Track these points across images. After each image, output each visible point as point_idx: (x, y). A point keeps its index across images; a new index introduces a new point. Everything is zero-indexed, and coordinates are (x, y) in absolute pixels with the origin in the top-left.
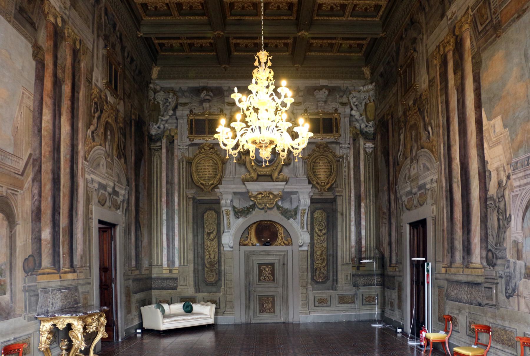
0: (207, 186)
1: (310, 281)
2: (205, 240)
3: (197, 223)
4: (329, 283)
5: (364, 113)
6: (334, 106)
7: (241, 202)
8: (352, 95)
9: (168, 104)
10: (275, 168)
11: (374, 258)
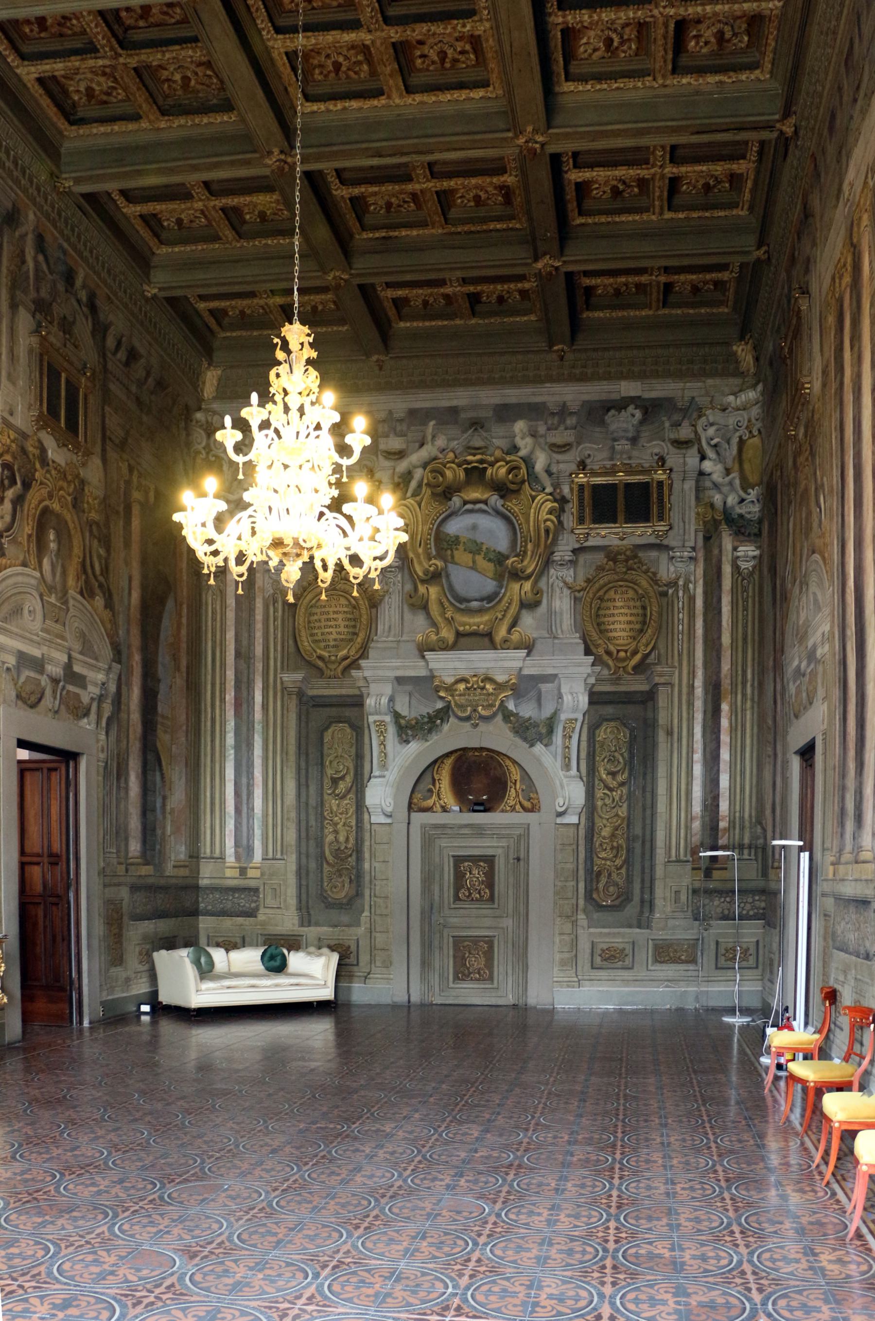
1: (581, 902)
2: (326, 797)
3: (307, 755)
4: (632, 910)
5: (736, 467)
6: (656, 450)
7: (413, 702)
8: (704, 419)
10: (500, 616)
11: (750, 847)
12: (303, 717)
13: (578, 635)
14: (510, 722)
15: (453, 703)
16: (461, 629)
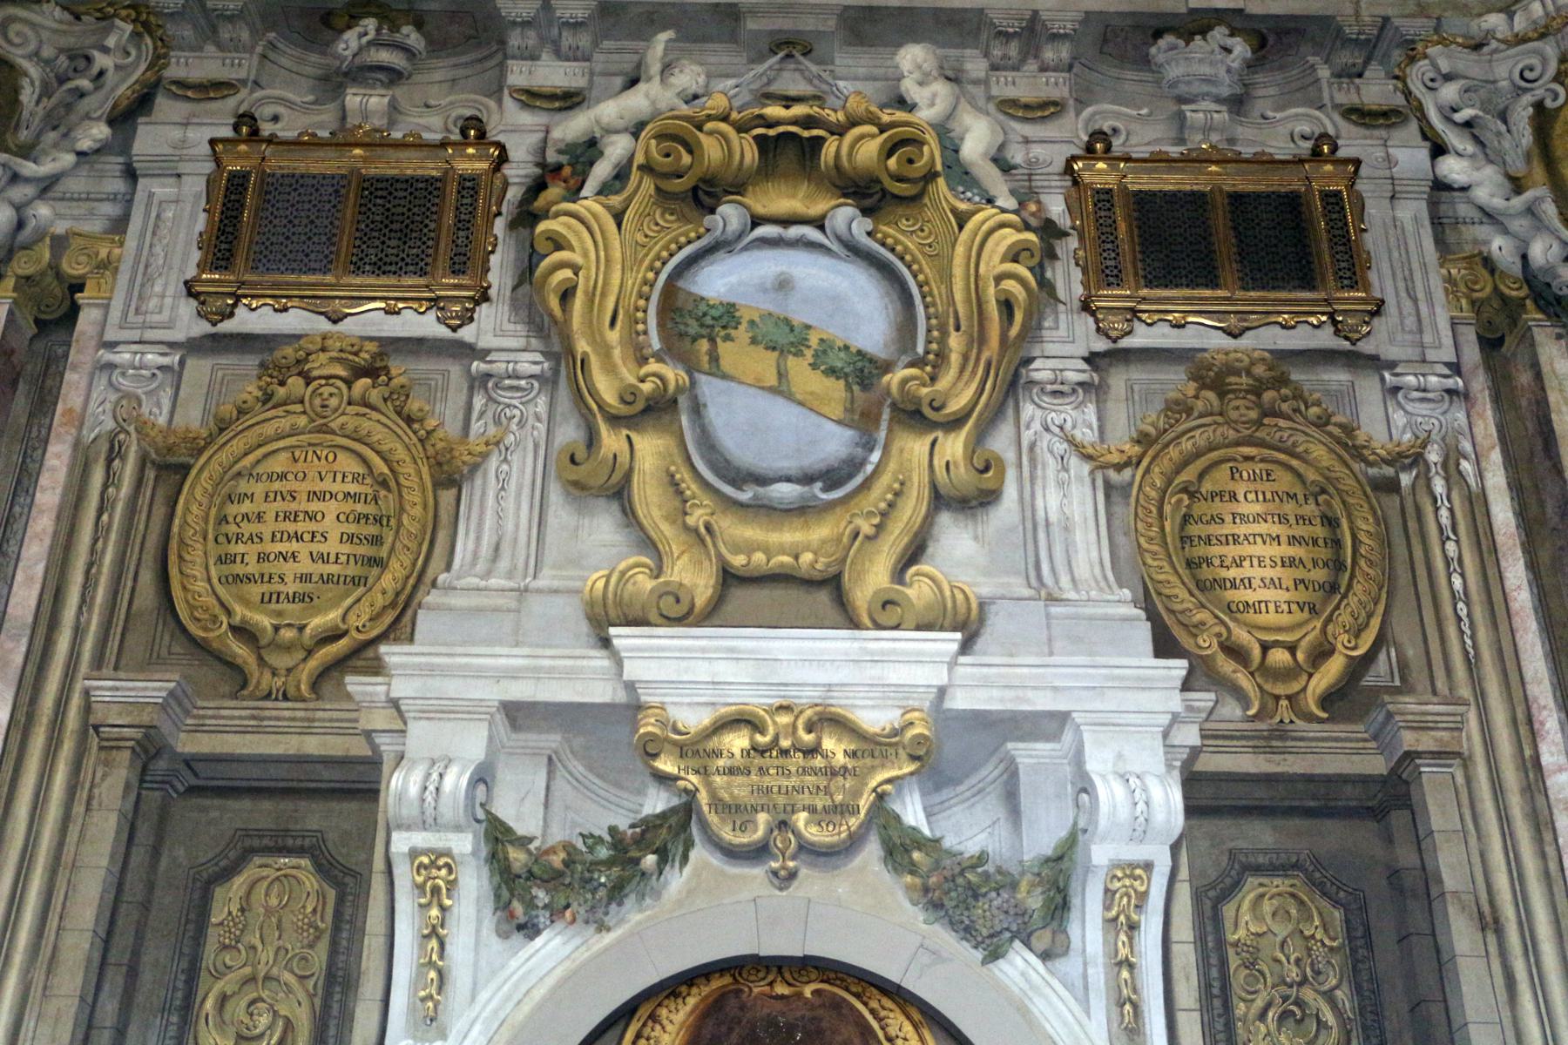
0: (288, 648)
3: (133, 973)
5: (1539, 172)
7: (560, 784)
9: (85, 83)
10: (866, 528)
12: (144, 832)
13: (1126, 593)
14: (913, 869)
15: (703, 797)
16: (738, 561)
